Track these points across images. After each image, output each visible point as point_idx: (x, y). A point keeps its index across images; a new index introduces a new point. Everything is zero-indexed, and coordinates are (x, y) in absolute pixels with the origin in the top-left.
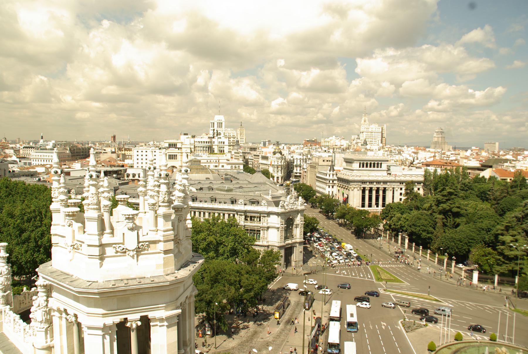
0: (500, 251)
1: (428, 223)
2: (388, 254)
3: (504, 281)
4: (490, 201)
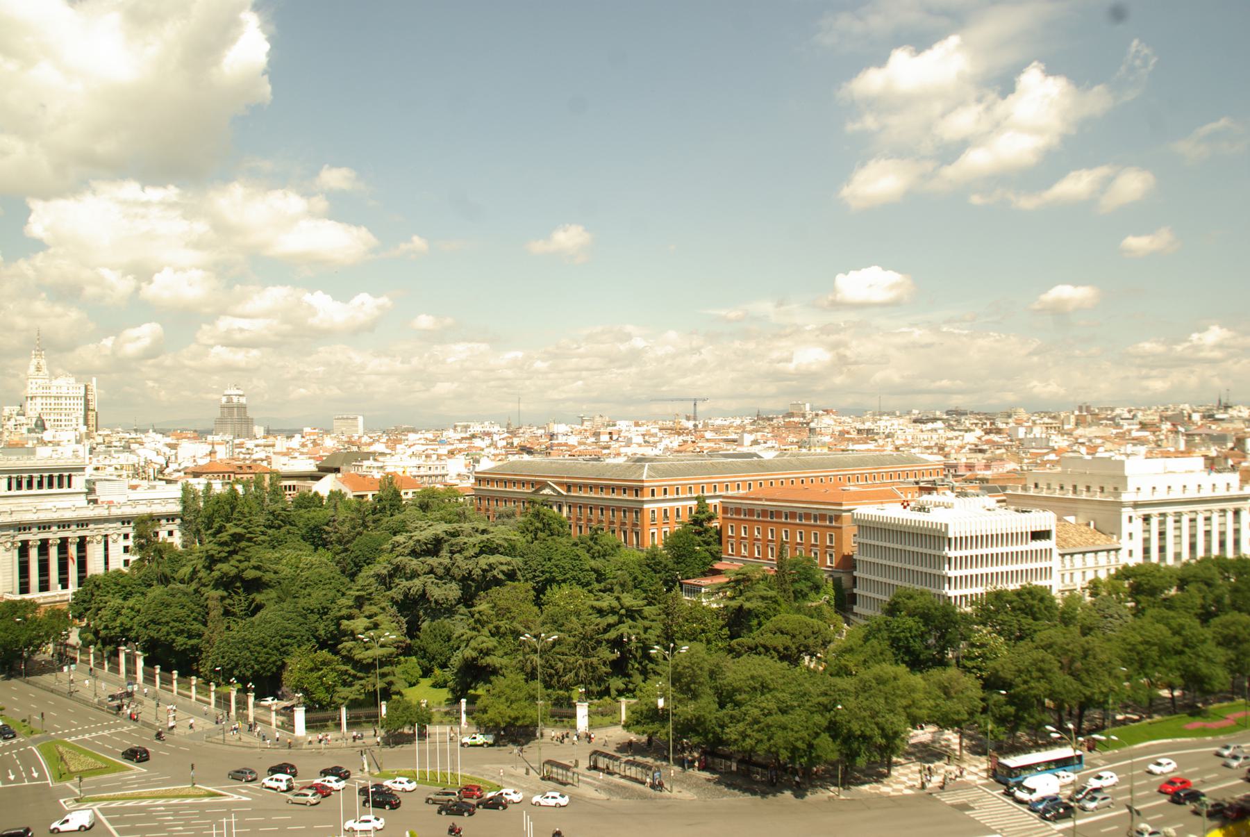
0: (344, 653)
1: (189, 612)
2: (92, 705)
3: (359, 717)
4: (330, 547)
